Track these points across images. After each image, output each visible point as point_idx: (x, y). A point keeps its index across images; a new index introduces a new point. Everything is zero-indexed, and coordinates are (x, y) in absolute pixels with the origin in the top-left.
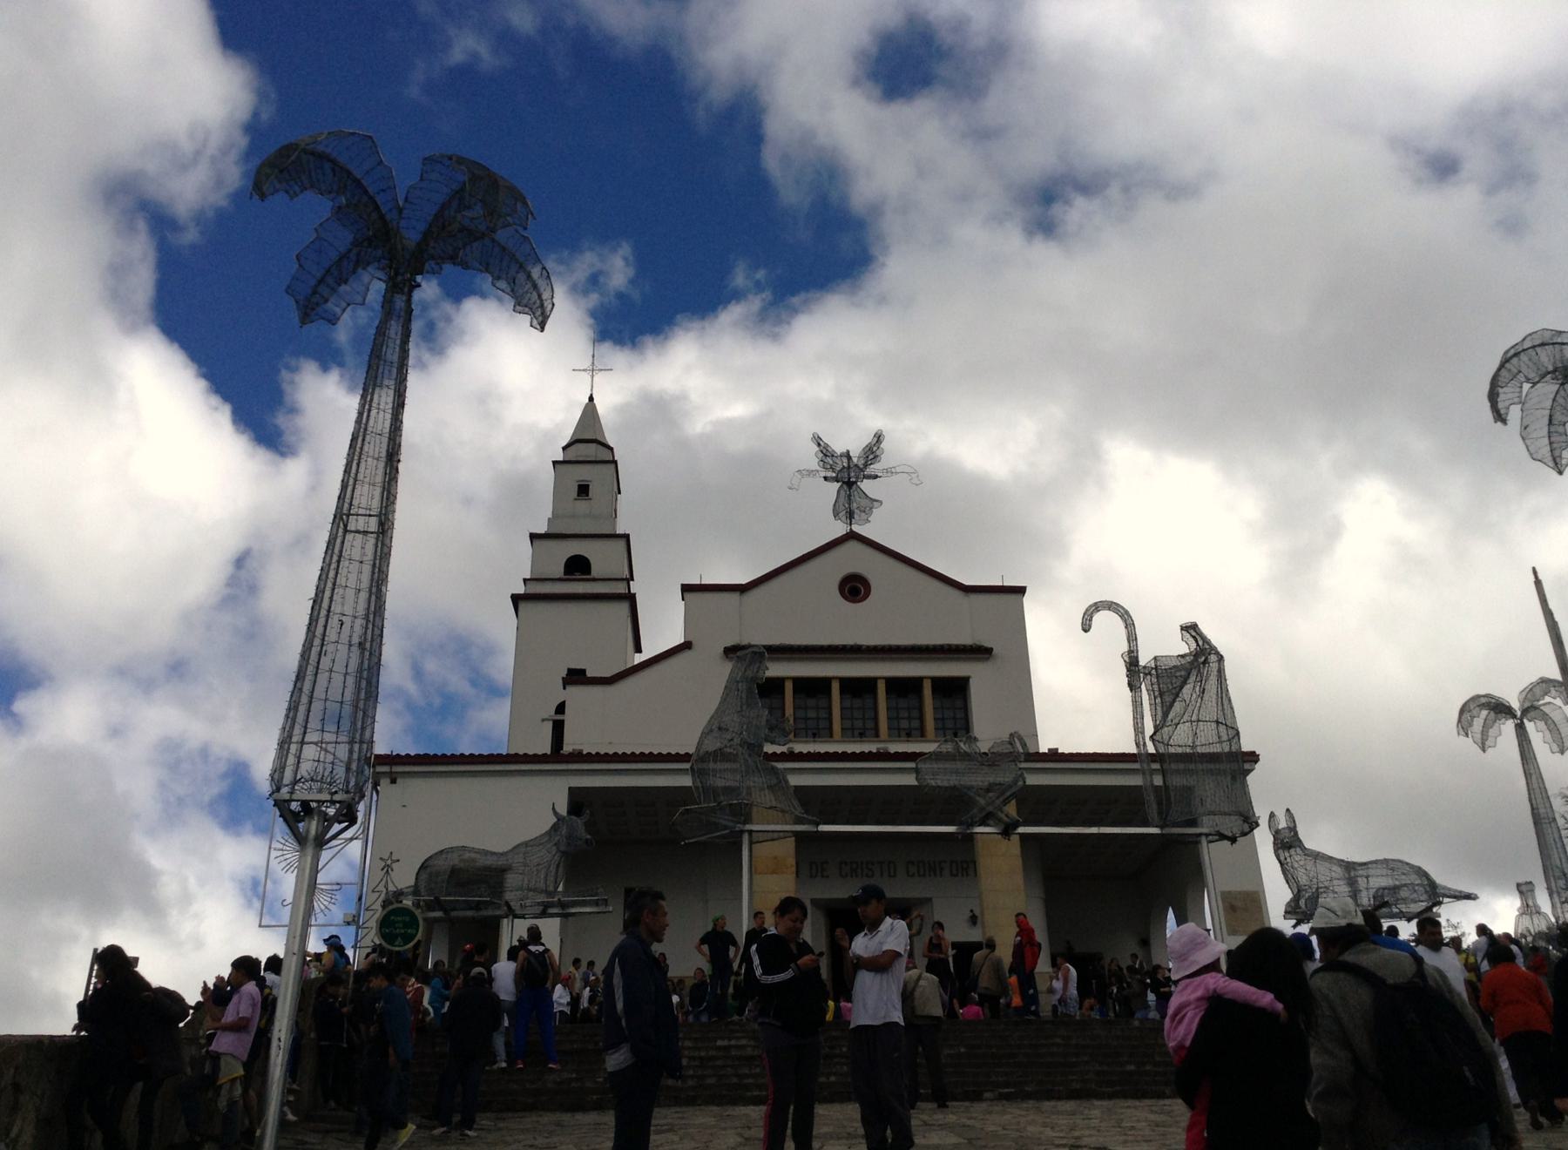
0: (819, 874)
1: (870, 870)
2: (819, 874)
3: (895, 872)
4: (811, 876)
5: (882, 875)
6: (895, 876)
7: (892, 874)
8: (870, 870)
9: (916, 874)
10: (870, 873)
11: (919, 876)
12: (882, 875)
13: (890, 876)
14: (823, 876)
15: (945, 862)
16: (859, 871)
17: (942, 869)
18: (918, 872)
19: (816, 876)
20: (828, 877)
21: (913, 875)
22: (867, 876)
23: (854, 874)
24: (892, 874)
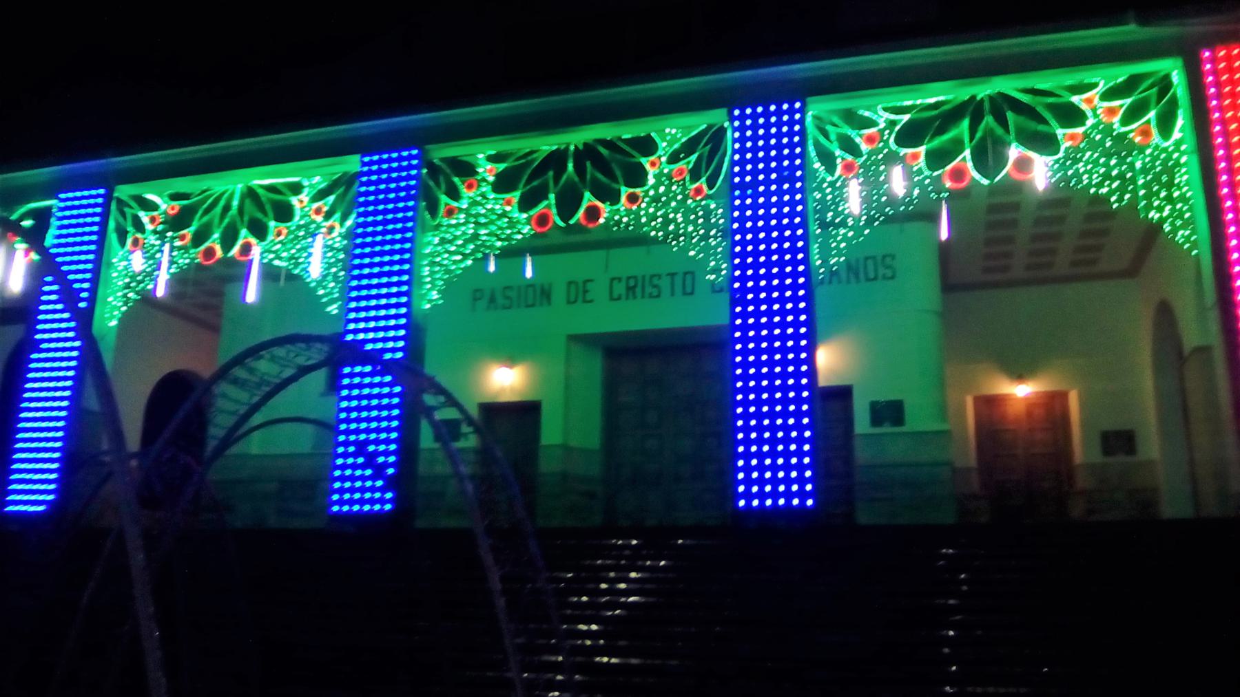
0: (580, 299)
1: (655, 286)
2: (580, 299)
4: (569, 302)
5: (673, 294)
6: (692, 293)
8: (655, 286)
10: (655, 292)
12: (673, 294)
13: (685, 293)
14: (585, 301)
16: (638, 290)
19: (575, 301)
20: (591, 301)
22: (651, 296)
23: (631, 294)
24: (689, 290)
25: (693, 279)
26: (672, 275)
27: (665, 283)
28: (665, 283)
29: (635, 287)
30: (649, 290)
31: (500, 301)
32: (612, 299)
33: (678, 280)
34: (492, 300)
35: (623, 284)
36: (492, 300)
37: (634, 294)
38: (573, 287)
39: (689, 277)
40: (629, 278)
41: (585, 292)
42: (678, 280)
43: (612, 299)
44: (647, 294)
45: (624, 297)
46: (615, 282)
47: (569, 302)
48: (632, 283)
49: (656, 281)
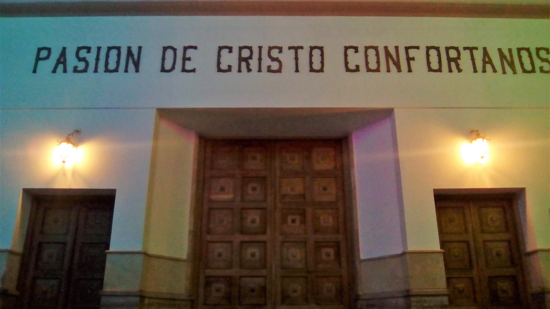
3: (322, 62)
4: (163, 70)
7: (317, 66)
9: (363, 68)
10: (275, 66)
11: (369, 70)
14: (184, 70)
15: (418, 48)
16: (254, 63)
17: (409, 59)
18: (367, 63)
19: (173, 68)
20: (194, 71)
21: (357, 69)
22: (269, 70)
23: (244, 64)
24: (317, 66)
25: (322, 55)
26: (296, 49)
27: (287, 57)
28: (287, 57)
29: (250, 57)
30: (266, 62)
31: (72, 61)
32: (220, 70)
33: (303, 55)
34: (62, 59)
35: (235, 53)
36: (62, 59)
37: (248, 65)
38: (170, 53)
39: (316, 53)
40: (241, 48)
41: (185, 59)
42: (303, 55)
43: (220, 70)
44: (264, 68)
45: (235, 68)
46: (225, 52)
47: (163, 70)
48: (246, 53)
49: (275, 53)
